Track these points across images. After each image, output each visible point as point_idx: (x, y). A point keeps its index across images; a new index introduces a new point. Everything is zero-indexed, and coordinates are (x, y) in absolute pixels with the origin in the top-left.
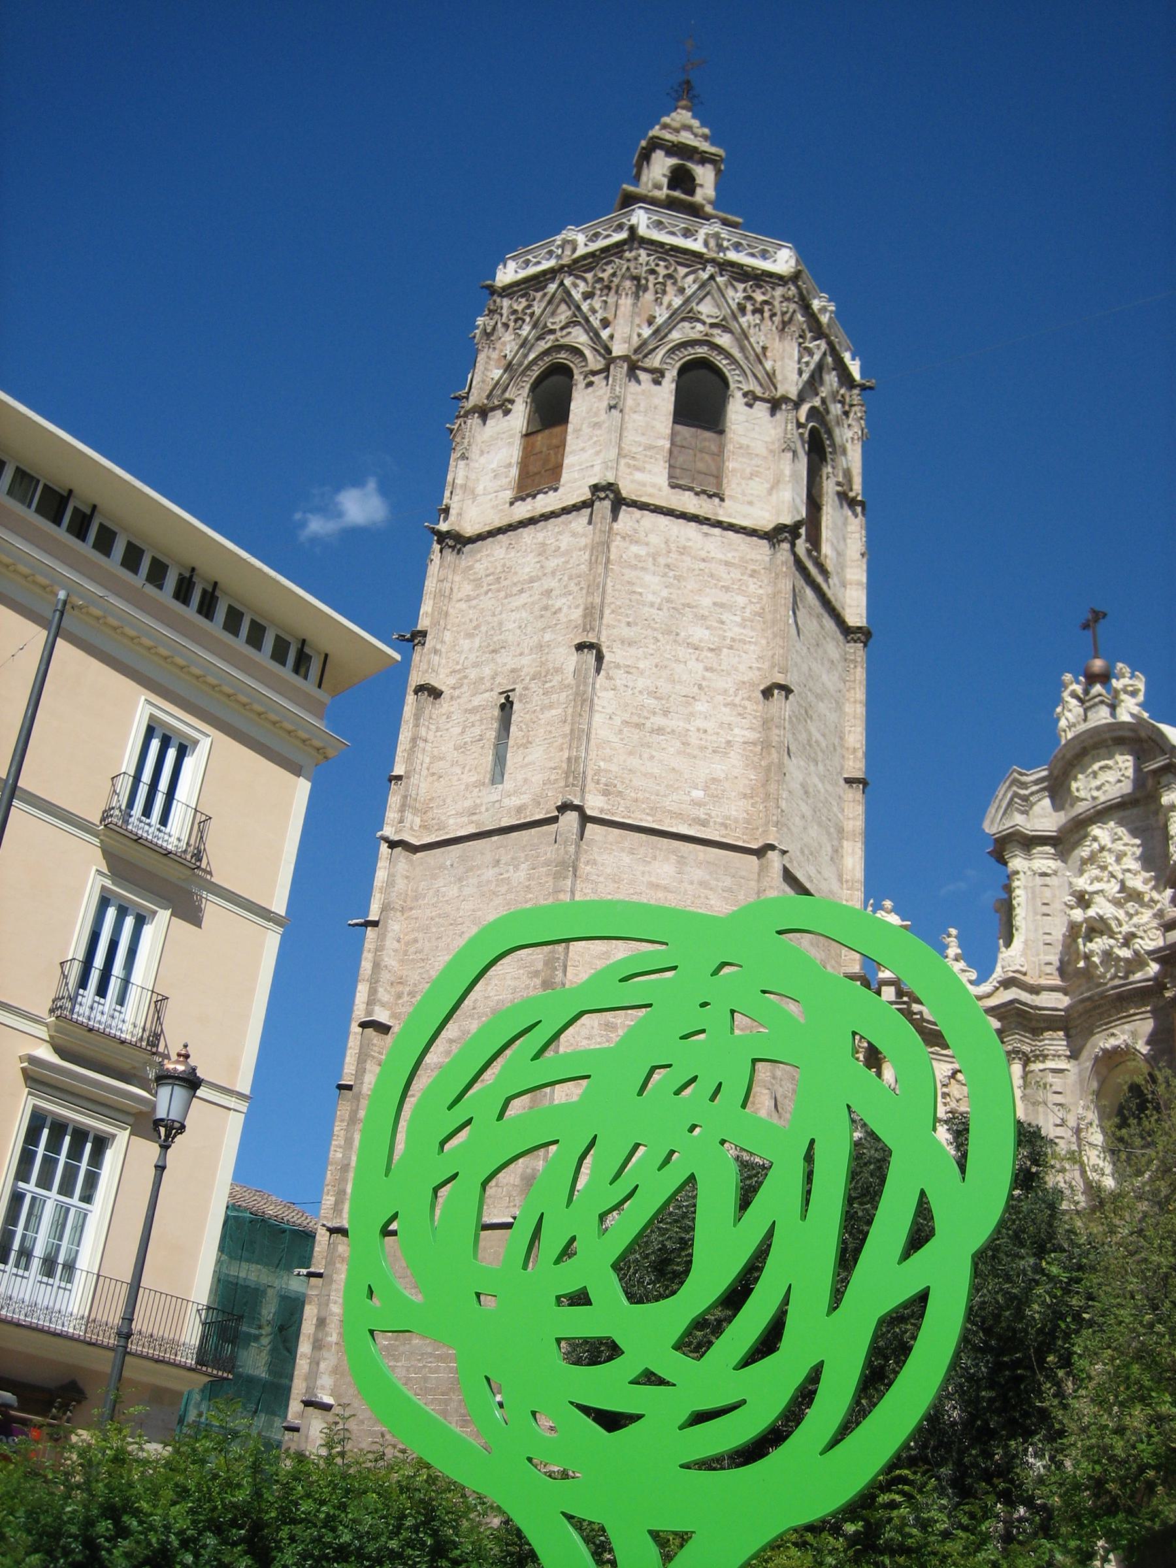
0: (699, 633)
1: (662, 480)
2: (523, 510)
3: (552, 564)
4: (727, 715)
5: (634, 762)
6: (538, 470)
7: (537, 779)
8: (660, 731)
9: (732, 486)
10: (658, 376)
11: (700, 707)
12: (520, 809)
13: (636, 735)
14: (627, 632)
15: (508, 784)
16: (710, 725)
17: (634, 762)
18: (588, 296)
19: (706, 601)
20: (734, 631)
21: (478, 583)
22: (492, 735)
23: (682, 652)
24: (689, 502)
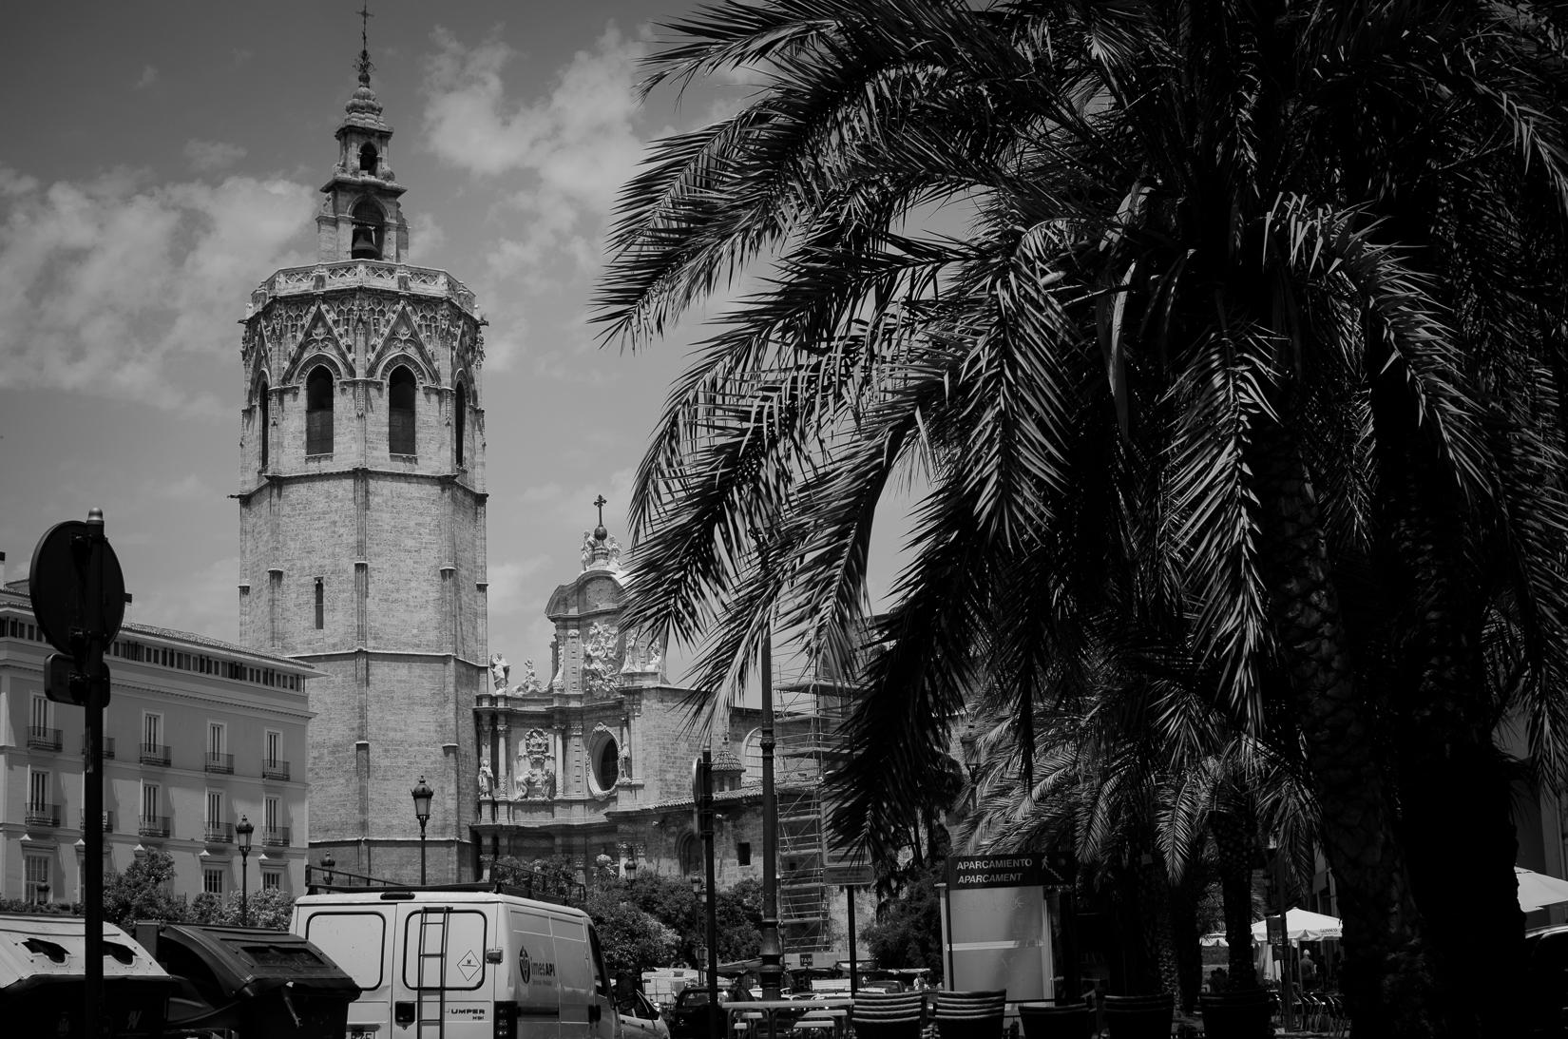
0: (410, 543)
1: (387, 454)
2: (314, 468)
3: (335, 505)
4: (425, 586)
5: (386, 620)
6: (320, 441)
7: (341, 630)
8: (395, 601)
9: (421, 449)
10: (379, 386)
11: (413, 584)
12: (334, 645)
13: (384, 605)
14: (376, 549)
15: (326, 630)
16: (418, 593)
17: (386, 620)
18: (335, 322)
19: (412, 524)
20: (426, 538)
21: (293, 507)
22: (313, 601)
23: (403, 555)
24: (401, 467)
